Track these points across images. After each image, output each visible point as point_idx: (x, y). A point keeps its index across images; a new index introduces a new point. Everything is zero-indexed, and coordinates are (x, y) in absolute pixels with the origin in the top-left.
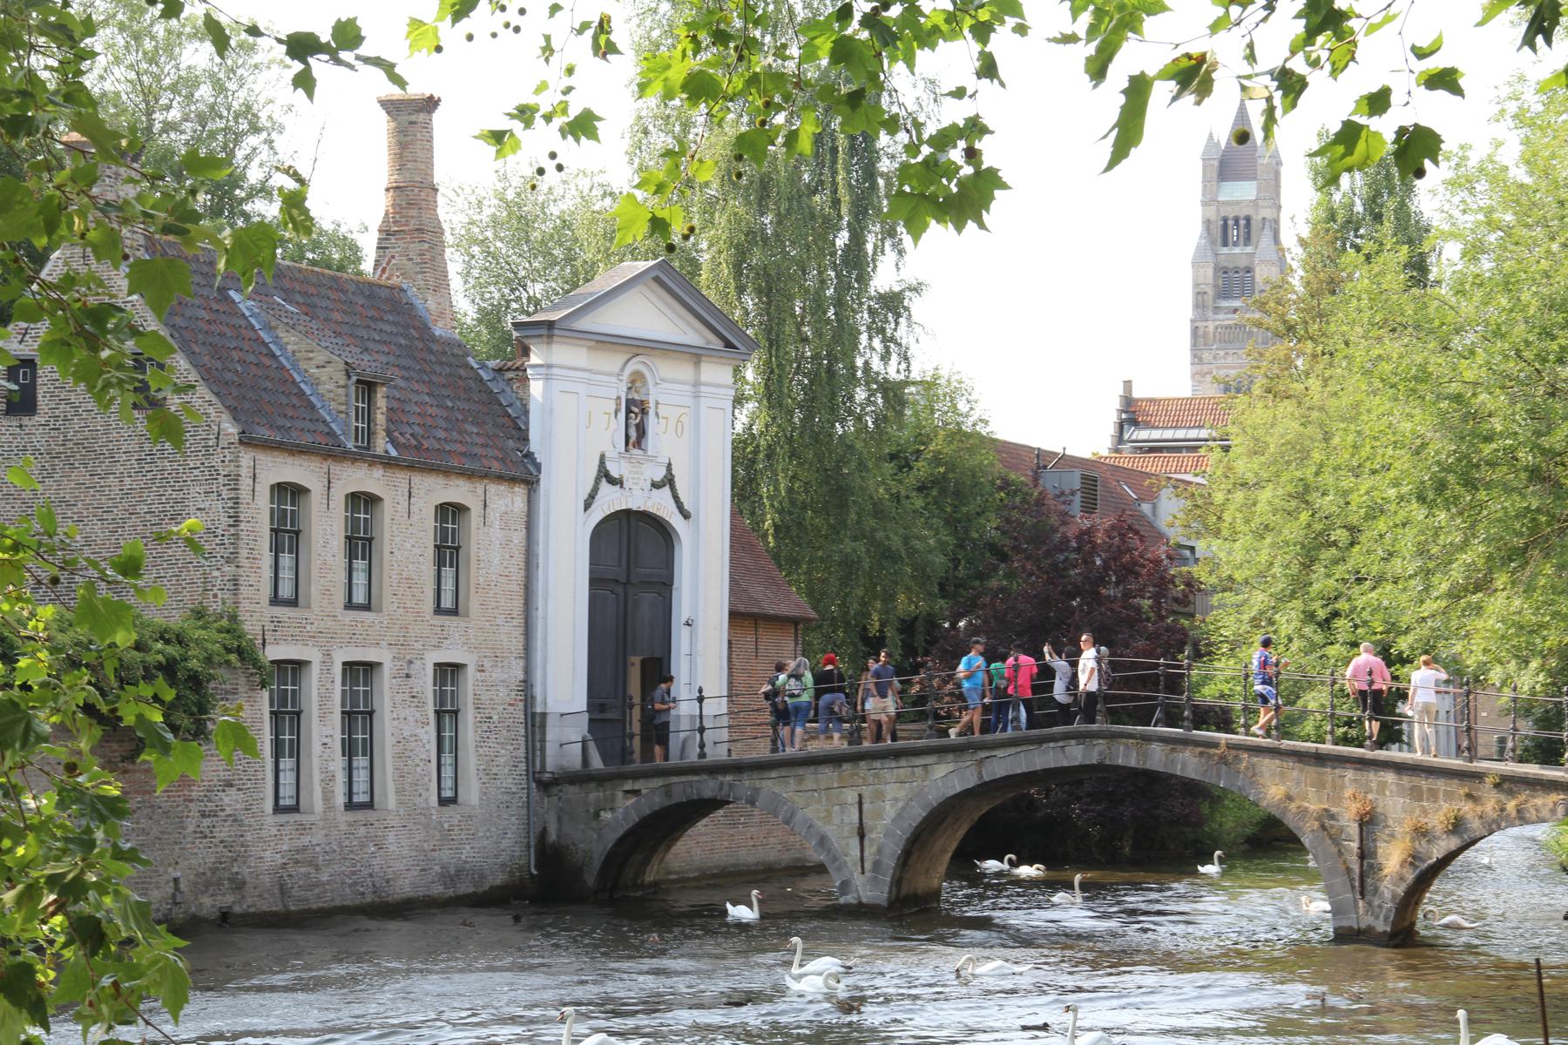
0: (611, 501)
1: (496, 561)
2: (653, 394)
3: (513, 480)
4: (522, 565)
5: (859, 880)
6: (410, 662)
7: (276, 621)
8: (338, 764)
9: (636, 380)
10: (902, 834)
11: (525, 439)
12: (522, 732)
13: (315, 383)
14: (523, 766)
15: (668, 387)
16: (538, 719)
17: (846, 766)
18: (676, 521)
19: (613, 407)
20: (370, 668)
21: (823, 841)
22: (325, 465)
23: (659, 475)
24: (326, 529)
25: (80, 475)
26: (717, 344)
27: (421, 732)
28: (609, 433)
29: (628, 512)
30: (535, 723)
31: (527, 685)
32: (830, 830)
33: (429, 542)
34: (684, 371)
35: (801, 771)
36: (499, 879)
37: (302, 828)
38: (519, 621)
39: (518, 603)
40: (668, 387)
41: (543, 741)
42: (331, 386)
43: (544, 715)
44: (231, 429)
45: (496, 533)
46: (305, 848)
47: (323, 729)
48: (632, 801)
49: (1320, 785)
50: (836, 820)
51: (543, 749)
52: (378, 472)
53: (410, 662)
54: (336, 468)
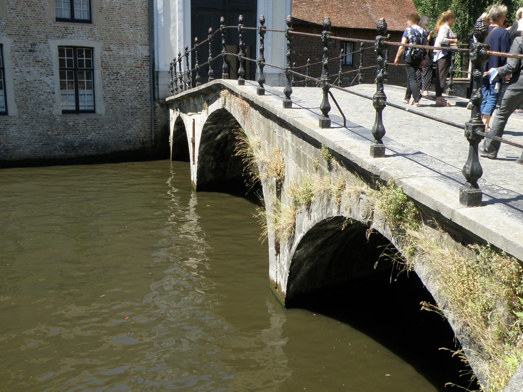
6: (33, 45)
12: (148, 80)
16: (155, 74)
27: (46, 79)
31: (151, 59)
39: (142, 20)
41: (158, 84)
43: (158, 72)
53: (33, 45)
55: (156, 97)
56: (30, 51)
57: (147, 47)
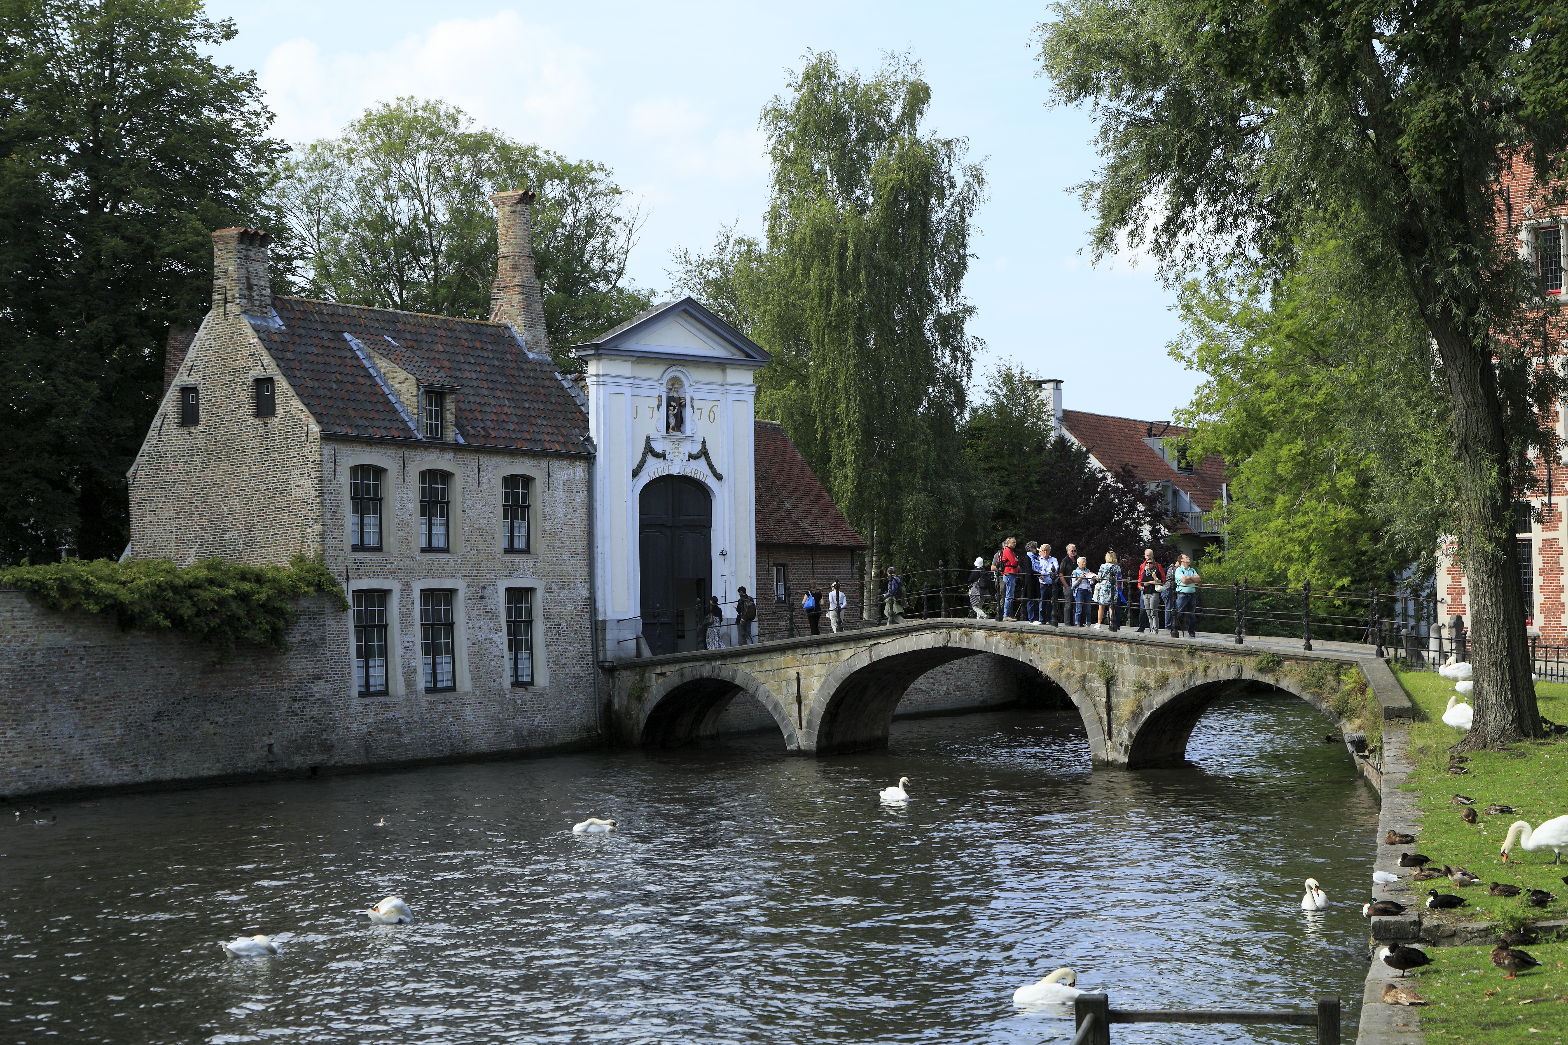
0: (654, 469)
1: (561, 514)
2: (688, 393)
3: (573, 457)
4: (585, 517)
5: (799, 734)
6: (484, 588)
7: (359, 564)
8: (419, 661)
9: (675, 382)
10: (825, 700)
11: (587, 429)
13: (398, 394)
14: (590, 658)
15: (698, 387)
17: (789, 653)
18: (711, 482)
19: (655, 402)
20: (449, 594)
21: (776, 705)
22: (400, 452)
23: (696, 449)
24: (402, 496)
25: (225, 465)
26: (739, 356)
28: (654, 422)
29: (671, 477)
30: (598, 628)
31: (592, 601)
32: (781, 699)
33: (499, 501)
34: (715, 376)
35: (761, 657)
36: (570, 738)
37: (386, 707)
38: (582, 556)
39: (582, 544)
40: (698, 387)
41: (604, 640)
42: (408, 396)
43: (604, 622)
44: (315, 429)
45: (560, 494)
46: (389, 721)
47: (405, 635)
48: (661, 680)
49: (1081, 656)
50: (784, 692)
51: (604, 646)
52: (449, 456)
53: (484, 588)
54: (409, 454)
55: (601, 658)
56: (482, 598)
57: (587, 585)
